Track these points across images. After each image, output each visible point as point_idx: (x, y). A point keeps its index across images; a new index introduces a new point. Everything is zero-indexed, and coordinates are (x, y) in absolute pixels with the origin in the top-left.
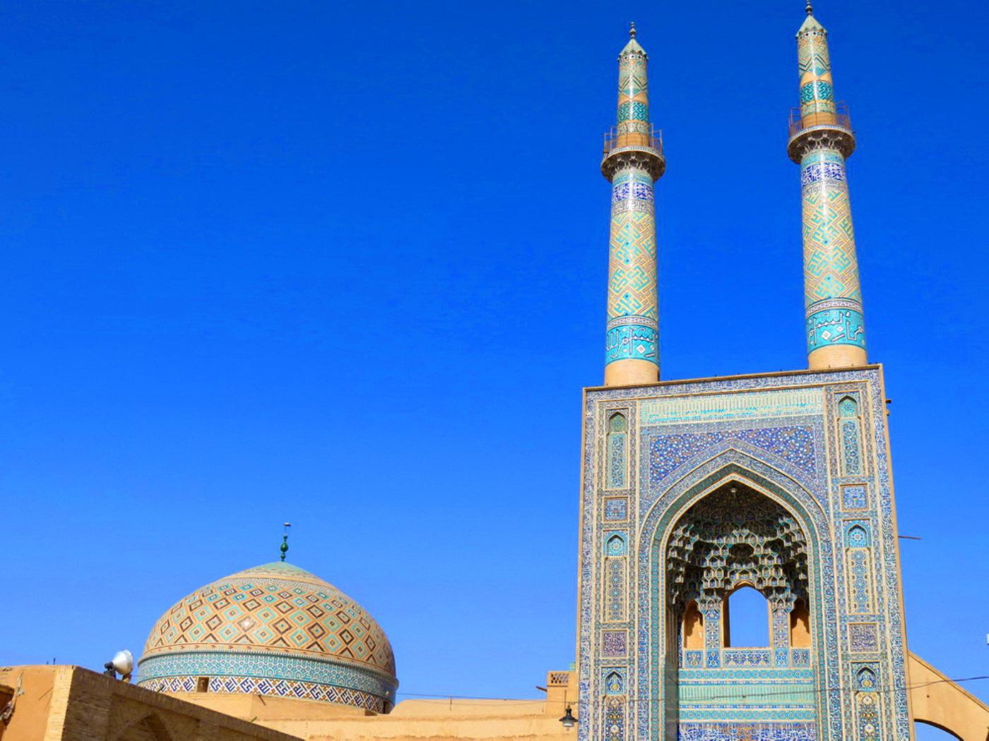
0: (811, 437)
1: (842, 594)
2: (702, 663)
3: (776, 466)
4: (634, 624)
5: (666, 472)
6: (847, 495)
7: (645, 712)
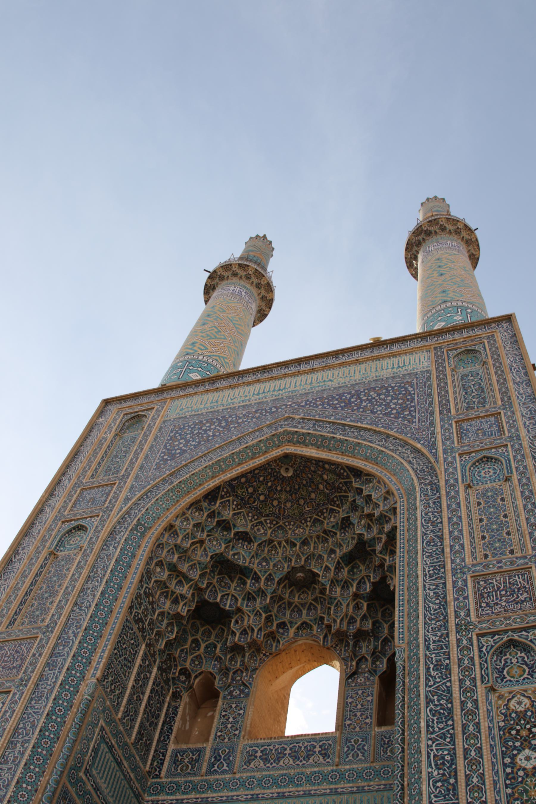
0: (410, 389)
1: (456, 539)
2: (200, 768)
3: (354, 421)
4: (54, 628)
5: (183, 452)
6: (467, 430)
7: (9, 769)
